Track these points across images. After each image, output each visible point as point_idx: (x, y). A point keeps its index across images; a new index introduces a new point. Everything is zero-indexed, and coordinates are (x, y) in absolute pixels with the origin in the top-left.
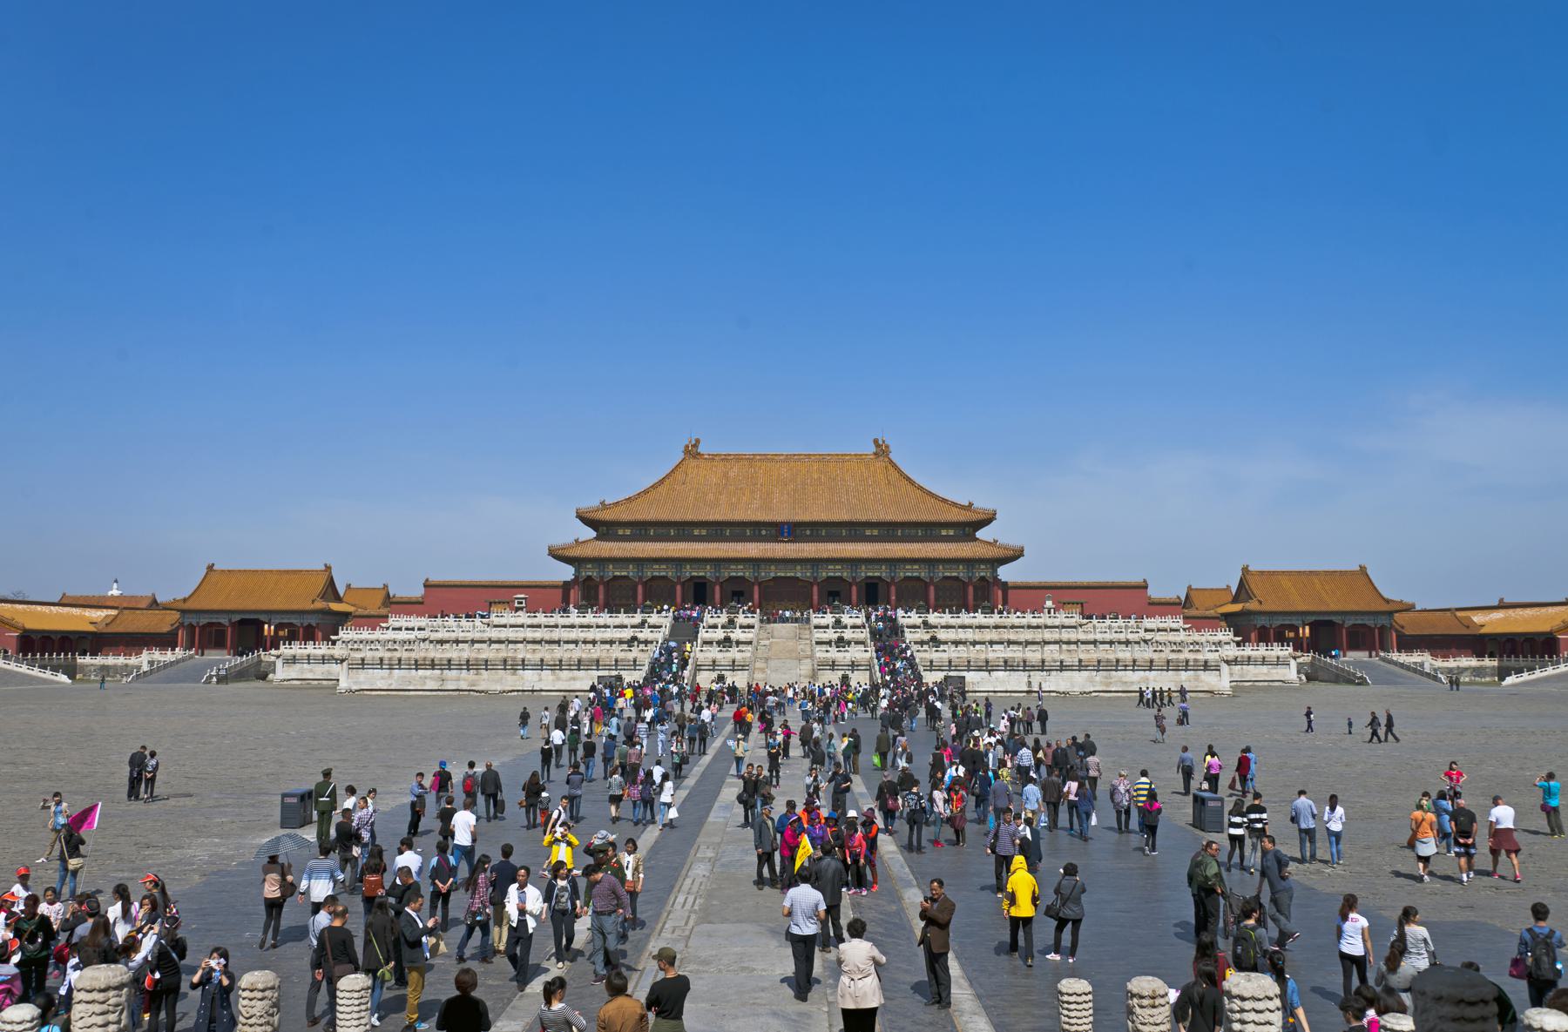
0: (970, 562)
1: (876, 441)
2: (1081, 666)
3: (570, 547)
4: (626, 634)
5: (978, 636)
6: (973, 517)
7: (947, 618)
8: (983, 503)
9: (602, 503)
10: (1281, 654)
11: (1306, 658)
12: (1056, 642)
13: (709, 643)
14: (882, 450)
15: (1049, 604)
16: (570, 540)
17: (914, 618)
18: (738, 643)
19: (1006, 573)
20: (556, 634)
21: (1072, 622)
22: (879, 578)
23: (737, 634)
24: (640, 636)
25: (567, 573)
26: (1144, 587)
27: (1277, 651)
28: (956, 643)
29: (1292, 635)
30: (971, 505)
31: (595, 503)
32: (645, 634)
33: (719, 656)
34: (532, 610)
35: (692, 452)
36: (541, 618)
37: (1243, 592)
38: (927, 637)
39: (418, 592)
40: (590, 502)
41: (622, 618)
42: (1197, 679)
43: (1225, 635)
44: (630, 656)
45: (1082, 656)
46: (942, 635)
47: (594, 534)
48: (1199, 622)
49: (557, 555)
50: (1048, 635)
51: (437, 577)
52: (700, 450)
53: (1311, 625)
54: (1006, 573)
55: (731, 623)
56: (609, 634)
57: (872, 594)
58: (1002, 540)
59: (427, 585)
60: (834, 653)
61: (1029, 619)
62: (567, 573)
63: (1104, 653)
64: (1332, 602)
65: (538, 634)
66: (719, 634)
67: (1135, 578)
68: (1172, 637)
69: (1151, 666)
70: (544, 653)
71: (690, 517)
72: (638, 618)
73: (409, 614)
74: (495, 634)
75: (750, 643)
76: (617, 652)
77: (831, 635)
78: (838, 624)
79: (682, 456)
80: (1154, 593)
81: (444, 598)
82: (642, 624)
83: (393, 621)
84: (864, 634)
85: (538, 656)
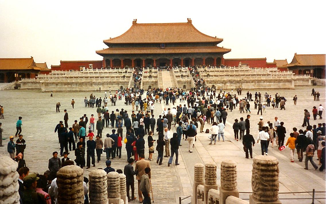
1: (188, 19)
3: (102, 51)
4: (123, 75)
5: (221, 74)
6: (217, 40)
7: (211, 69)
8: (219, 37)
9: (110, 38)
10: (306, 78)
11: (313, 79)
12: (244, 75)
13: (145, 77)
15: (240, 65)
16: (102, 49)
17: (202, 69)
18: (154, 77)
19: (226, 56)
20: (103, 75)
21: (247, 69)
23: (153, 74)
24: (126, 75)
25: (101, 58)
26: (265, 59)
27: (305, 77)
28: (215, 76)
29: (309, 72)
31: (109, 38)
32: (127, 75)
33: (149, 80)
34: (94, 68)
35: (135, 23)
36: (97, 70)
37: (294, 60)
38: (206, 75)
39: (58, 64)
40: (107, 38)
41: (120, 70)
42: (285, 85)
43: (289, 73)
44: (124, 81)
46: (211, 74)
47: (108, 47)
48: (282, 69)
50: (241, 73)
51: (63, 60)
52: (137, 22)
53: (314, 70)
54: (226, 56)
55: (151, 71)
56: (118, 75)
57: (187, 63)
58: (225, 47)
59: (61, 62)
60: (180, 79)
61: (235, 69)
62: (101, 58)
63: (257, 78)
65: (98, 75)
66: (148, 74)
67: (263, 57)
68: (274, 73)
69: (270, 81)
70: (100, 80)
72: (124, 70)
73: (57, 70)
74: (84, 75)
76: (121, 80)
77: (179, 74)
78: (180, 71)
79: (132, 24)
80: (268, 61)
81: (66, 66)
82: (126, 72)
83: (53, 72)
84: (188, 73)
85: (98, 81)
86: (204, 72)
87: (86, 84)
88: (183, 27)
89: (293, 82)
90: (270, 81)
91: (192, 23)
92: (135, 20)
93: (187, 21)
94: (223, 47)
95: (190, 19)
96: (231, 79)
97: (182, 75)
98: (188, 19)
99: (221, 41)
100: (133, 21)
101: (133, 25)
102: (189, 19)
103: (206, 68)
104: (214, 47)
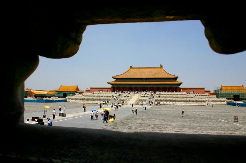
2: (182, 101)
3: (110, 82)
8: (177, 75)
14: (161, 67)
25: (110, 86)
31: (115, 75)
35: (131, 67)
45: (183, 99)
49: (108, 83)
51: (92, 87)
56: (109, 95)
59: (91, 88)
64: (236, 92)
69: (193, 101)
70: (98, 98)
80: (206, 90)
87: (90, 100)
88: (158, 69)
89: (206, 102)
90: (193, 101)
93: (160, 66)
103: (161, 93)
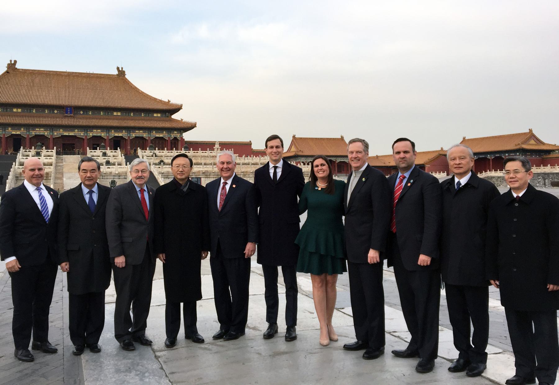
0: (170, 130)
1: (118, 68)
8: (175, 101)
14: (121, 73)
19: (188, 136)
22: (122, 137)
26: (249, 144)
30: (169, 101)
38: (157, 161)
52: (18, 66)
54: (188, 136)
61: (208, 153)
71: (11, 100)
75: (51, 165)
78: (105, 154)
79: (6, 69)
80: (254, 147)
86: (152, 156)
91: (126, 76)
92: (13, 62)
94: (182, 120)
95: (122, 68)
96: (206, 169)
97: (108, 163)
98: (118, 68)
99: (177, 109)
100: (9, 64)
101: (7, 72)
102: (120, 69)
103: (157, 152)
104: (167, 119)
